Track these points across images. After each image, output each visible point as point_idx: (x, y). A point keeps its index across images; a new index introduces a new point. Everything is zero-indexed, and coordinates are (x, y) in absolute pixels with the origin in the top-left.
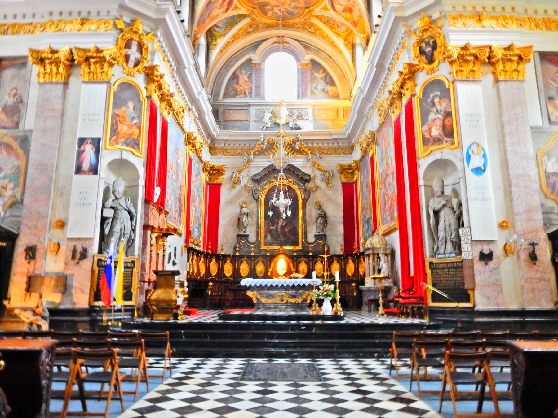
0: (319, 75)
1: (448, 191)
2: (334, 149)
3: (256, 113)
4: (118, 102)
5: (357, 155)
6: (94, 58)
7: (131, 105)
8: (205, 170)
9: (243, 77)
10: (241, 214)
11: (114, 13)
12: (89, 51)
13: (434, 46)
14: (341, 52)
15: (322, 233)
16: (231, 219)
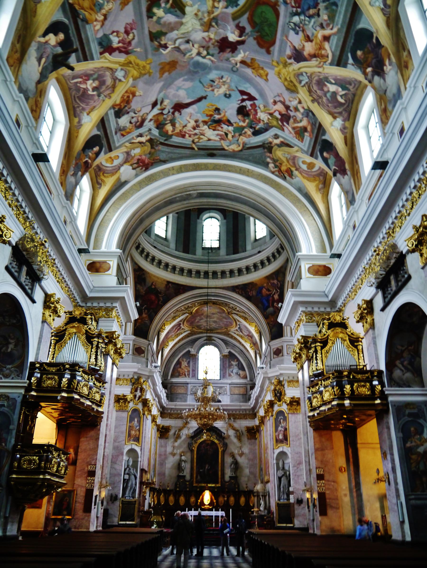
0: (234, 363)
1: (286, 468)
2: (243, 415)
3: (192, 389)
4: (131, 419)
5: (257, 422)
6: (121, 399)
7: (136, 420)
8: (158, 430)
9: (184, 364)
10: (181, 461)
11: (131, 376)
12: (120, 395)
13: (281, 394)
14: (248, 351)
15: (234, 475)
16: (173, 465)
